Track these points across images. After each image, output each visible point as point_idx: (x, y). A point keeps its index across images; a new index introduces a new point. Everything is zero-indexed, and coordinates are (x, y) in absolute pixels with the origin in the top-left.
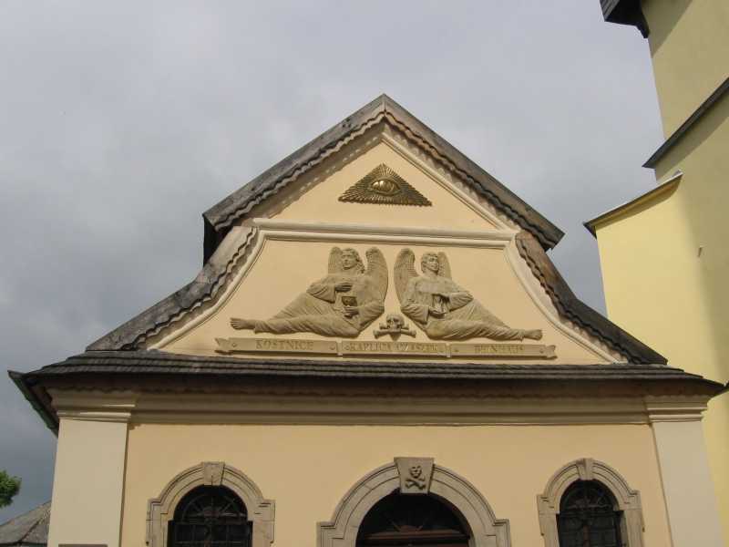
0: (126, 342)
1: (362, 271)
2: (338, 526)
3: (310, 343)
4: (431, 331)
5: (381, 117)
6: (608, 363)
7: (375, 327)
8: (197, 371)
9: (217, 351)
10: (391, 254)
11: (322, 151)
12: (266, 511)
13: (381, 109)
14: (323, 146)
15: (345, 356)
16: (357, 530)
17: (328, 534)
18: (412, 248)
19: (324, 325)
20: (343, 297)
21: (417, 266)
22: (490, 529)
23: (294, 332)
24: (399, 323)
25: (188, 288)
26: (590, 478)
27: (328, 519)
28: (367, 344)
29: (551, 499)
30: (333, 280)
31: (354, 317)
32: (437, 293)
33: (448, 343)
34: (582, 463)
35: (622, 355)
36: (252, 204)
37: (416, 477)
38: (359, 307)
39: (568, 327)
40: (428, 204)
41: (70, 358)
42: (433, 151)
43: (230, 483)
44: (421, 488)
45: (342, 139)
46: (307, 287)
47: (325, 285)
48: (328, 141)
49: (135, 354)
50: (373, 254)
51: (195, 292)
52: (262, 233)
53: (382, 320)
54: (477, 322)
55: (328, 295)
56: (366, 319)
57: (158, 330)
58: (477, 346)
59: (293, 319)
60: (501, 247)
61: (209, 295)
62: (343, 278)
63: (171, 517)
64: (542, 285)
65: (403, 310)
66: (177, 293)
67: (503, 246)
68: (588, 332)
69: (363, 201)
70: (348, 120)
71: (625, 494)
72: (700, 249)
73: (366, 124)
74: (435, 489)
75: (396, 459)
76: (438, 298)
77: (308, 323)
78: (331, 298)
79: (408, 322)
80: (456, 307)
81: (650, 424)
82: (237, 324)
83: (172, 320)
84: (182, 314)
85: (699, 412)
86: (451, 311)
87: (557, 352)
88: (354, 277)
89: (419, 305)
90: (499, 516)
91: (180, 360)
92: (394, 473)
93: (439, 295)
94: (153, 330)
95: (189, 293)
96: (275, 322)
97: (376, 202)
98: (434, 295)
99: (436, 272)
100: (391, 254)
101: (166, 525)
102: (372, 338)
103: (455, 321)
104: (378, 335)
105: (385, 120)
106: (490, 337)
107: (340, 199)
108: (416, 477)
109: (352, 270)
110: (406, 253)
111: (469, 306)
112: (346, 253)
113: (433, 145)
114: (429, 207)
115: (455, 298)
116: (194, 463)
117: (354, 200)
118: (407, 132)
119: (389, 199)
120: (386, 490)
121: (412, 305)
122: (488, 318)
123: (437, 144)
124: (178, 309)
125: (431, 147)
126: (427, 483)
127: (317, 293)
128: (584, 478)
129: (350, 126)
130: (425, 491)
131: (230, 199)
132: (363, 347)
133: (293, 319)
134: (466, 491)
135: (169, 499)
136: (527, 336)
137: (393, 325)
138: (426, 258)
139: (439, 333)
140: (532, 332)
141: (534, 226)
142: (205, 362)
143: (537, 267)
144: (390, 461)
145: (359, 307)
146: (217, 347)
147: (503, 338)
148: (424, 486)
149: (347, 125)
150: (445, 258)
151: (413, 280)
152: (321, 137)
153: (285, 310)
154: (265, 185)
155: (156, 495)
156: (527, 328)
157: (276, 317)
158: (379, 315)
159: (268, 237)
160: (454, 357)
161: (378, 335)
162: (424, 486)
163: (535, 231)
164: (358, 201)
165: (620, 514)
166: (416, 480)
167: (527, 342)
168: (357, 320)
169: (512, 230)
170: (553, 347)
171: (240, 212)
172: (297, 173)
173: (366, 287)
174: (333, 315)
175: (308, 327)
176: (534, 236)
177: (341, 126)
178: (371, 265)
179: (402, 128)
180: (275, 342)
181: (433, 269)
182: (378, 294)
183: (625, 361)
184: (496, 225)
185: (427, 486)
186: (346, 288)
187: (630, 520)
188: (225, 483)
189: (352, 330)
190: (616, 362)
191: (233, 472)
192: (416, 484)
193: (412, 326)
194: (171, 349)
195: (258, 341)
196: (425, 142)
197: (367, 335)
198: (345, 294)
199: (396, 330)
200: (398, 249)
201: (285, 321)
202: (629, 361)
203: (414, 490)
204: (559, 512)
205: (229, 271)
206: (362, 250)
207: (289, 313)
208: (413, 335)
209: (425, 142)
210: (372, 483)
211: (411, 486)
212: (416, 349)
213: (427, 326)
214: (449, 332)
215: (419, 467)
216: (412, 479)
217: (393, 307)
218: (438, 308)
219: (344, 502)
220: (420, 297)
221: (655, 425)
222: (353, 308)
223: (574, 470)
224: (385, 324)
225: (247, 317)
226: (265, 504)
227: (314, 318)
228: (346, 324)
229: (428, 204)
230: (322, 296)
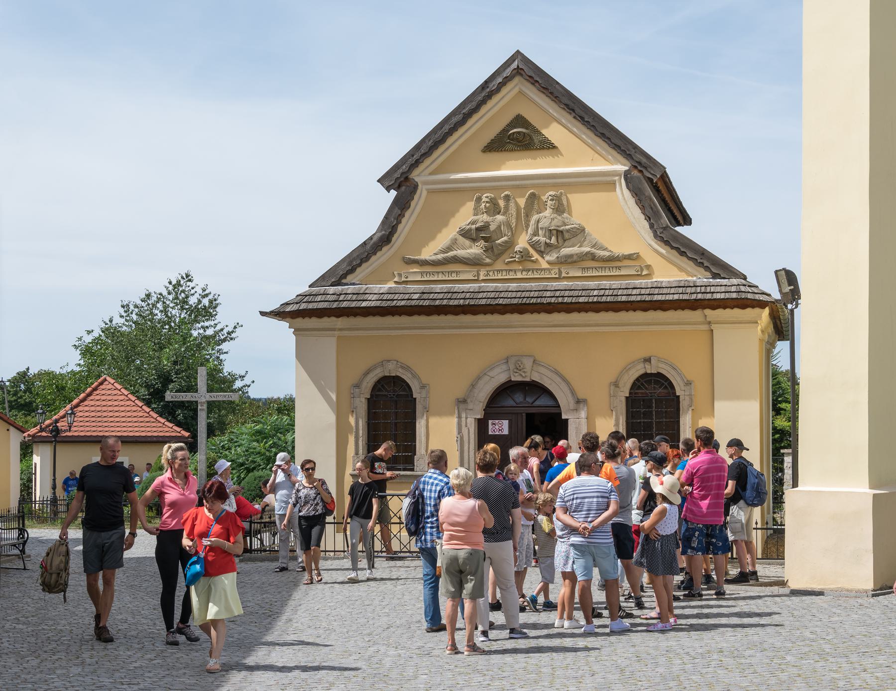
0: (333, 280)
1: (499, 214)
2: (469, 401)
8: (373, 304)
17: (462, 406)
22: (572, 405)
25: (371, 238)
30: (473, 223)
34: (648, 360)
41: (298, 296)
46: (458, 230)
47: (468, 227)
52: (425, 187)
54: (586, 249)
56: (499, 252)
65: (529, 243)
71: (682, 384)
74: (536, 378)
79: (532, 251)
89: (539, 238)
90: (581, 396)
96: (434, 258)
101: (363, 400)
121: (535, 238)
128: (649, 372)
130: (528, 379)
132: (496, 273)
134: (558, 380)
136: (629, 257)
141: (640, 163)
169: (622, 167)
174: (475, 250)
175: (457, 260)
177: (481, 88)
186: (485, 227)
193: (536, 256)
199: (525, 256)
201: (440, 257)
203: (519, 379)
212: (535, 273)
219: (473, 386)
227: (460, 253)
230: (467, 235)
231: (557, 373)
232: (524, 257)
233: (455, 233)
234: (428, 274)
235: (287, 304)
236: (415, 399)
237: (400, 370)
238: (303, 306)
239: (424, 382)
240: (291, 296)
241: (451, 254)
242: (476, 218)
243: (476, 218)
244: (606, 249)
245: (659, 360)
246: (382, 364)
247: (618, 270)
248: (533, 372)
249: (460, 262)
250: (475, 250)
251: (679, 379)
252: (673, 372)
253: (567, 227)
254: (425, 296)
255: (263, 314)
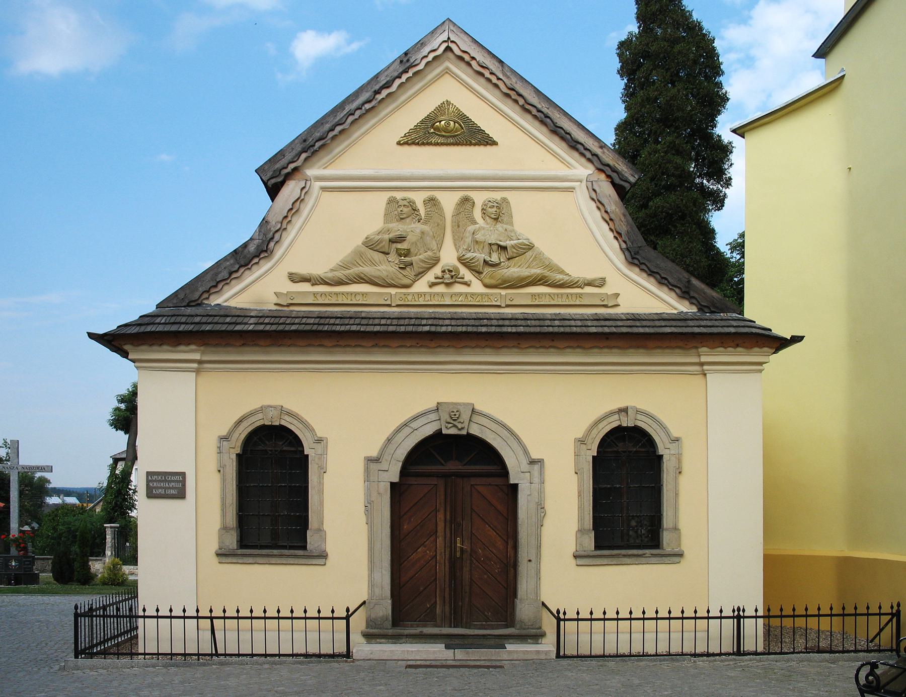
3: (364, 294)
4: (488, 281)
5: (444, 46)
6: (675, 312)
7: (430, 277)
9: (275, 304)
10: (449, 202)
11: (377, 92)
12: (319, 448)
13: (444, 37)
14: (377, 87)
15: (398, 306)
16: (400, 464)
17: (374, 467)
18: (472, 195)
19: (378, 278)
20: (397, 249)
21: (477, 214)
22: (525, 466)
23: (347, 284)
24: (453, 274)
25: (245, 245)
26: (631, 424)
27: (374, 453)
28: (419, 294)
29: (589, 441)
30: (388, 231)
31: (408, 269)
32: (494, 242)
33: (503, 292)
34: (624, 410)
35: (692, 303)
36: (304, 156)
37: (454, 420)
38: (414, 259)
39: (635, 274)
40: (494, 143)
42: (500, 83)
43: (287, 422)
44: (460, 430)
45: (399, 77)
48: (383, 80)
49: (199, 311)
50: (432, 202)
51: (252, 248)
52: (318, 184)
53: (437, 271)
54: (537, 271)
55: (384, 246)
56: (421, 270)
57: (220, 286)
58: (533, 295)
59: (348, 272)
60: (571, 190)
61: (266, 251)
62: (398, 228)
63: (238, 450)
64: (611, 229)
66: (235, 251)
67: (574, 188)
68: (656, 279)
69: (423, 144)
70: (406, 54)
72: (850, 169)
73: (426, 57)
74: (475, 430)
75: (438, 403)
76: (495, 248)
77: (362, 275)
78: (386, 251)
79: (464, 272)
80: (515, 255)
81: (705, 375)
82: (295, 278)
83: (233, 276)
84: (242, 270)
85: (761, 364)
86: (509, 259)
87: (620, 300)
88: (412, 229)
89: (475, 255)
90: (535, 455)
91: (242, 315)
92: (433, 416)
93: (497, 244)
94: (216, 286)
95: (246, 251)
96: (330, 275)
97: (437, 144)
98: (490, 244)
99: (496, 219)
100: (449, 202)
101: (234, 457)
102: (426, 289)
103: (514, 270)
104: (432, 285)
105: (448, 49)
106: (549, 286)
107: (399, 143)
108: (454, 420)
109: (408, 220)
110: (466, 200)
111: (530, 253)
112: (401, 203)
113: (501, 76)
114: (494, 147)
115: (513, 247)
116: (257, 406)
117: (414, 143)
118: (473, 63)
119: (451, 140)
120: (429, 430)
122: (551, 267)
123: (505, 74)
124: (237, 266)
125: (499, 79)
126: (466, 425)
127: (371, 244)
129: (408, 61)
130: (464, 432)
131: (281, 154)
133: (348, 272)
134: (505, 433)
135: (235, 435)
136: (590, 284)
137: (447, 276)
138: (485, 205)
139: (493, 282)
140: (595, 280)
141: (608, 165)
142: (261, 316)
143: (606, 212)
144: (432, 405)
145: (414, 259)
146: (276, 300)
147: (562, 286)
148: (463, 428)
149: (405, 60)
150: (508, 203)
151: (471, 228)
152: (377, 77)
153: (341, 264)
154: (318, 135)
155: (224, 433)
156: (590, 276)
157: (332, 270)
158: (435, 265)
159: (324, 189)
160: (508, 306)
161: (432, 285)
162: (463, 428)
163: (609, 172)
164: (418, 144)
165: (660, 457)
166: (454, 423)
167: (588, 290)
168: (408, 271)
170: (617, 295)
171: (292, 166)
172: (351, 119)
173: (421, 238)
174: (386, 267)
175: (363, 279)
176: (608, 176)
178: (427, 214)
179: (467, 58)
180: (330, 294)
181: (493, 216)
182: (434, 245)
183: (694, 309)
184: (569, 166)
185: (466, 427)
186: (400, 239)
187: (668, 465)
188: (283, 423)
189: (406, 281)
190: (685, 310)
191: (290, 414)
192: (455, 426)
193: (467, 275)
194: (233, 303)
195: (315, 294)
196: (492, 73)
197: (421, 286)
198: (399, 246)
200: (457, 196)
201: (339, 274)
202: (700, 310)
203: (453, 431)
204: (596, 455)
205: (284, 226)
206: (419, 198)
207: (344, 266)
208: (467, 284)
209: (492, 73)
210: (414, 425)
211: (451, 427)
212: (470, 299)
213: (482, 276)
214: (504, 282)
215: (457, 411)
216: (452, 422)
217: (449, 256)
218: (495, 258)
219: (389, 440)
220: (477, 247)
221: (708, 375)
222: (407, 259)
223: (616, 417)
224: (440, 274)
225: (304, 271)
226: (319, 441)
227: (368, 270)
228: (400, 276)
229: (494, 143)
230: (375, 249)
231: (504, 426)
232: (455, 277)
233: (360, 243)
234: (323, 295)
235: (126, 325)
236: (308, 455)
237: (286, 417)
238: (149, 329)
239: (320, 434)
240: (133, 317)
241: (354, 271)
242: (391, 225)
243: (391, 225)
244: (562, 272)
245: (638, 411)
246: (262, 409)
247: (578, 298)
248: (471, 422)
249: (367, 282)
250: (386, 267)
251: (663, 435)
252: (655, 425)
253: (512, 242)
254: (322, 321)
255: (91, 336)
